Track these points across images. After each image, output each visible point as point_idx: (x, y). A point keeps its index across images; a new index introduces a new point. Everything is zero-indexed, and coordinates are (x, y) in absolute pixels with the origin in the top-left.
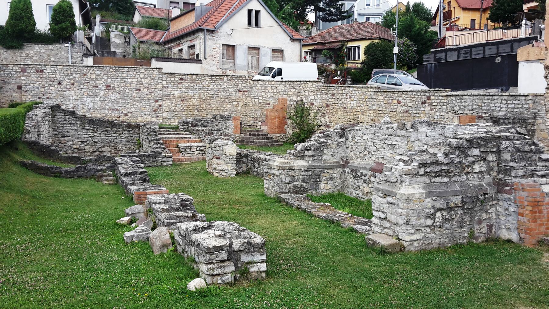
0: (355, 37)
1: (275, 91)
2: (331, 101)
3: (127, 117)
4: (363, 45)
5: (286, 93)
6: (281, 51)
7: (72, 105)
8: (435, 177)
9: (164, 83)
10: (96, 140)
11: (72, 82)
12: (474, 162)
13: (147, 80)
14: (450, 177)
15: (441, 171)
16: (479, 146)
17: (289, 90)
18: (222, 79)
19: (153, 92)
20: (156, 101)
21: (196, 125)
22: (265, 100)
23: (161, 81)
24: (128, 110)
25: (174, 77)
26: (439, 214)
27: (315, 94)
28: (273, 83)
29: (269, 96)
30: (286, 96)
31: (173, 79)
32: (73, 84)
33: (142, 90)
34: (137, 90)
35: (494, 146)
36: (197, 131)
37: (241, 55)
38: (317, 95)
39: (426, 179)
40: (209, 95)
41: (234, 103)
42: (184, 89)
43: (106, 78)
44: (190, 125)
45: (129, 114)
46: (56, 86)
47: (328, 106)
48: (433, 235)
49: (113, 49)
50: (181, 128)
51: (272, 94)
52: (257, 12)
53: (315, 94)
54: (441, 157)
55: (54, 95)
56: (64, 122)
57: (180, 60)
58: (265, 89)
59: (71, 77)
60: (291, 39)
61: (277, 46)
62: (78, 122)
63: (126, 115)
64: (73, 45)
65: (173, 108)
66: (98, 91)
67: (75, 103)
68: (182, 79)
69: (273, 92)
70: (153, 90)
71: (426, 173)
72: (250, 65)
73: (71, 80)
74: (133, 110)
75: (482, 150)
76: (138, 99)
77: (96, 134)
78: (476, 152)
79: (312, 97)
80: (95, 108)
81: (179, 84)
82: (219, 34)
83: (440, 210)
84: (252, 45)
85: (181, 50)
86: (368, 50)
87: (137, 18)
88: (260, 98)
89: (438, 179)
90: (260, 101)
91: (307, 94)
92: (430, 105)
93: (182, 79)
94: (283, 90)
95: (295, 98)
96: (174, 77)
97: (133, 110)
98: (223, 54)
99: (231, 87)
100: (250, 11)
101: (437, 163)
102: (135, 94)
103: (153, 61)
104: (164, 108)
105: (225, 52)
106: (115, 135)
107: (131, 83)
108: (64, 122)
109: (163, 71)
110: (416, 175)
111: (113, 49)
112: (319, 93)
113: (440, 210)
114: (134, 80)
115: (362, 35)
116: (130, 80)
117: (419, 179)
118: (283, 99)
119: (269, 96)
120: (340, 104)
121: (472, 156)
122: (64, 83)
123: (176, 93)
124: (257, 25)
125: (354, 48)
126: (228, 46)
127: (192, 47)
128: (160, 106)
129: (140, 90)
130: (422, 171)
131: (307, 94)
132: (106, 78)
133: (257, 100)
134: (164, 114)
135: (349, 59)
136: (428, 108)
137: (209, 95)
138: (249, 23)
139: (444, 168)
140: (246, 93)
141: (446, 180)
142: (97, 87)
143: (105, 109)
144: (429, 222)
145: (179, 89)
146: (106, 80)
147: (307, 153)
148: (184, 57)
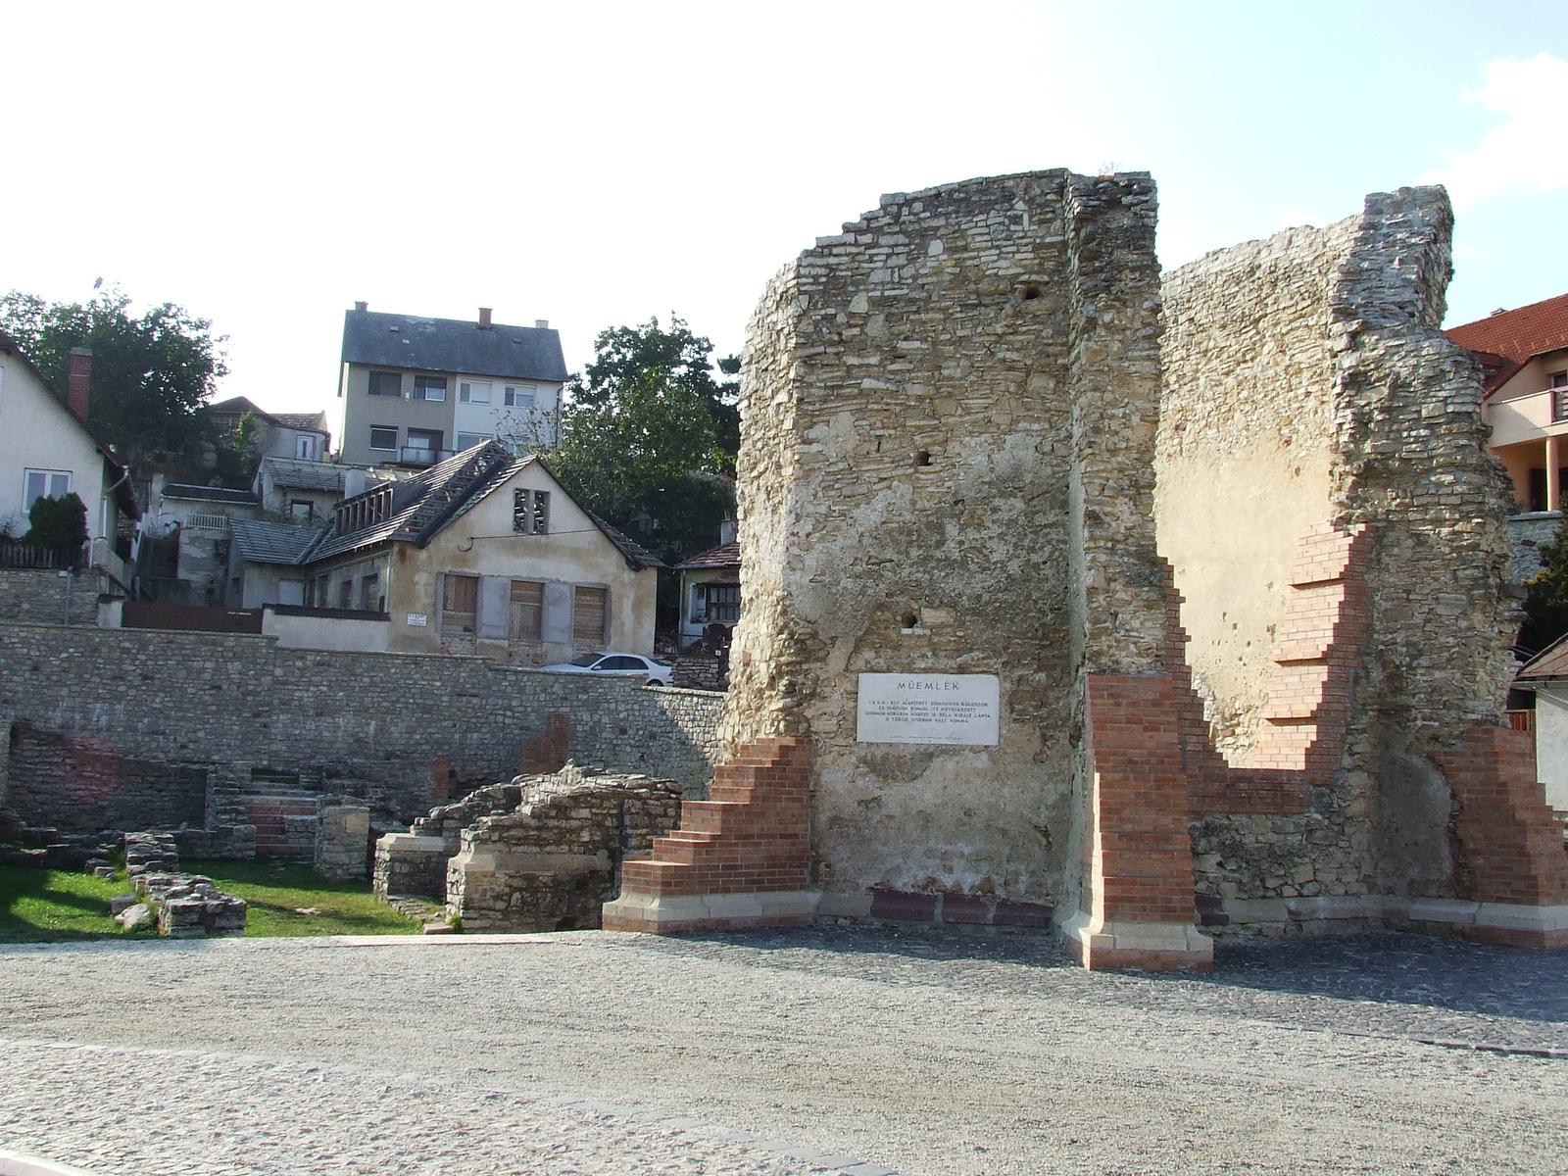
1: (542, 697)
3: (186, 751)
5: (568, 703)
6: (603, 593)
7: (59, 721)
8: (516, 845)
10: (105, 803)
11: (65, 665)
12: (582, 828)
14: (541, 846)
15: (526, 838)
19: (249, 693)
20: (257, 715)
21: (336, 775)
22: (518, 718)
23: (271, 668)
24: (190, 735)
26: (517, 895)
27: (629, 707)
28: (539, 678)
29: (530, 709)
30: (568, 709)
33: (225, 687)
34: (213, 687)
35: (615, 807)
36: (335, 786)
37: (491, 604)
38: (632, 709)
39: (500, 846)
40: (384, 704)
41: (445, 724)
42: (325, 689)
43: (144, 658)
44: (324, 774)
45: (191, 746)
46: (27, 675)
47: (653, 736)
48: (507, 923)
49: (183, 574)
50: (303, 779)
51: (535, 704)
52: (542, 497)
53: (629, 707)
55: (20, 695)
56: (37, 760)
57: (343, 612)
58: (521, 691)
59: (64, 655)
61: (591, 578)
62: (68, 761)
63: (183, 747)
65: (297, 732)
66: (122, 689)
68: (319, 664)
69: (538, 700)
70: (251, 688)
71: (501, 839)
73: (62, 660)
74: (201, 734)
75: (594, 810)
76: (214, 708)
77: (105, 789)
78: (585, 813)
80: (109, 728)
83: (519, 889)
88: (509, 713)
89: (521, 849)
91: (613, 706)
94: (561, 693)
97: (201, 734)
98: (446, 598)
99: (438, 684)
100: (520, 495)
105: (452, 595)
106: (149, 792)
108: (37, 760)
109: (279, 644)
110: (486, 840)
111: (183, 574)
112: (636, 707)
113: (519, 889)
114: (208, 665)
117: (491, 846)
118: (559, 717)
119: (530, 709)
121: (579, 819)
126: (461, 578)
127: (372, 579)
128: (265, 726)
129: (219, 688)
130: (495, 836)
131: (613, 706)
132: (144, 658)
133: (500, 719)
134: (274, 748)
137: (384, 704)
138: (519, 525)
139: (532, 833)
140: (475, 700)
141: (535, 849)
142: (122, 679)
144: (501, 905)
145: (312, 688)
146: (143, 663)
147: (446, 823)
148: (354, 608)
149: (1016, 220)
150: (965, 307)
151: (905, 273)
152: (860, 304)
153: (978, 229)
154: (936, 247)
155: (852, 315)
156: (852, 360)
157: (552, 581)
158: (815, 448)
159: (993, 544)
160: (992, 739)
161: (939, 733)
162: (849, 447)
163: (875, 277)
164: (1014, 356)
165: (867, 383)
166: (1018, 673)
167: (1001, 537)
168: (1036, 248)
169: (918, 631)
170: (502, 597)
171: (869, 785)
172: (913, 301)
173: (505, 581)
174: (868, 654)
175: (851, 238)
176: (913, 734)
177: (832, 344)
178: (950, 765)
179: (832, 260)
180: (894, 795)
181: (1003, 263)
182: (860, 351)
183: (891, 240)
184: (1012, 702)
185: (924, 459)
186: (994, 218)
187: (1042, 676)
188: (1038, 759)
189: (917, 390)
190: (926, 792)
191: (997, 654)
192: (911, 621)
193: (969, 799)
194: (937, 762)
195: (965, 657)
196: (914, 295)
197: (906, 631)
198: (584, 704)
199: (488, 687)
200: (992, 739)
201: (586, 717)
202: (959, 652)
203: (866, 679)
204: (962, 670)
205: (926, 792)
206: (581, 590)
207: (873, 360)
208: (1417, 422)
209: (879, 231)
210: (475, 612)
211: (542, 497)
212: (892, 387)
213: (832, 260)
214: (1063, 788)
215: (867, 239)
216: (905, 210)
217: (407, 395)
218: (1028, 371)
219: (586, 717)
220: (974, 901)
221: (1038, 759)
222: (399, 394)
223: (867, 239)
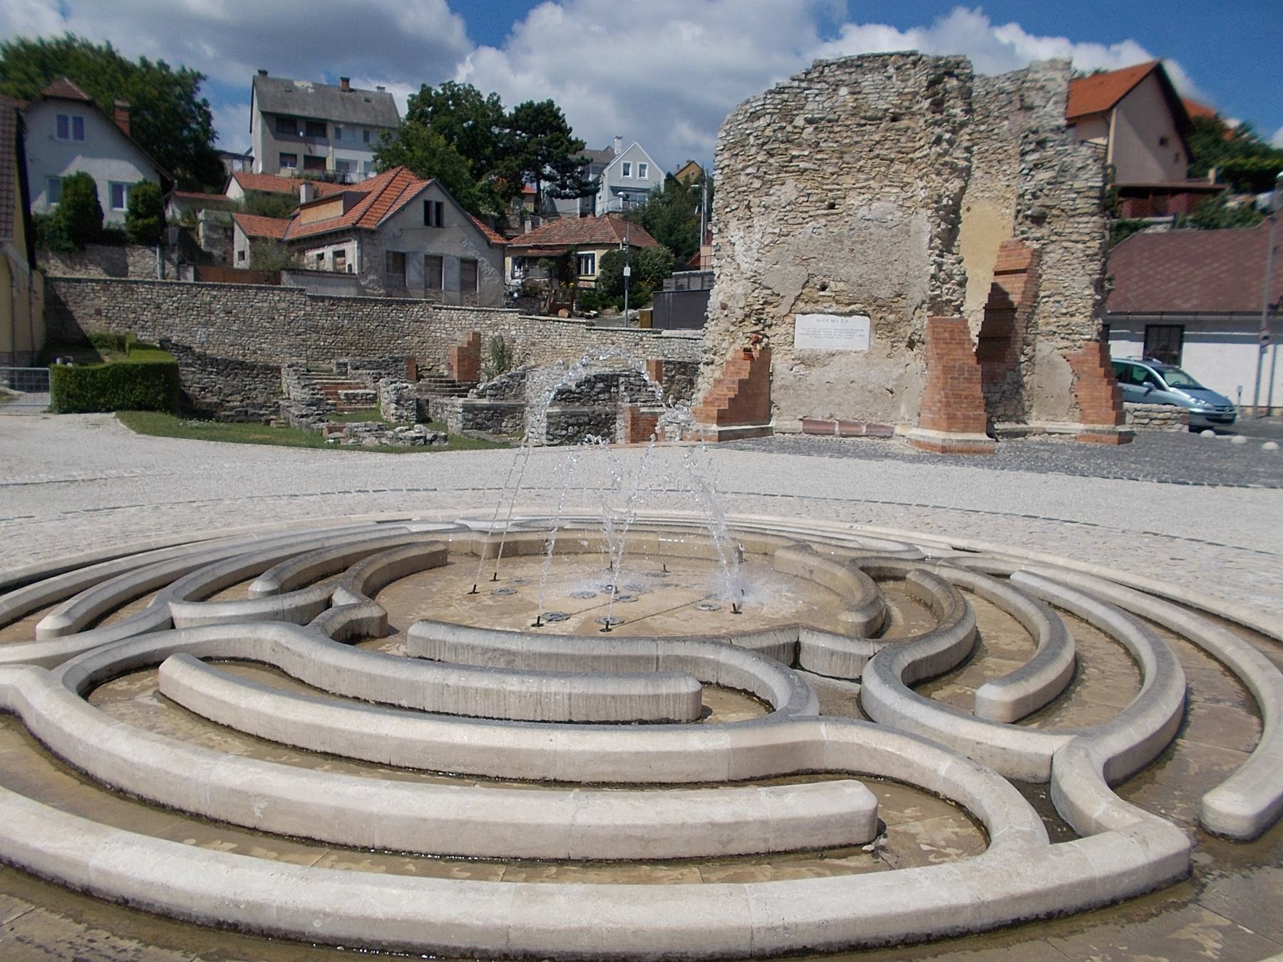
0: (587, 240)
2: (537, 338)
4: (599, 254)
6: (475, 262)
9: (308, 309)
13: (283, 305)
16: (602, 381)
32: (177, 308)
47: (533, 344)
52: (439, 205)
54: (573, 388)
58: (451, 319)
61: (471, 254)
78: (601, 385)
85: (321, 257)
86: (604, 260)
87: (234, 192)
92: (643, 347)
95: (490, 333)
101: (570, 391)
105: (391, 262)
115: (599, 238)
120: (548, 342)
122: (164, 307)
123: (325, 323)
124: (439, 223)
125: (587, 257)
135: (579, 272)
136: (641, 351)
138: (427, 221)
149: (890, 78)
150: (860, 125)
151: (826, 105)
152: (799, 121)
153: (869, 81)
154: (843, 91)
155: (795, 127)
156: (795, 153)
158: (774, 198)
159: (870, 252)
160: (865, 347)
161: (838, 344)
162: (793, 198)
163: (809, 107)
164: (885, 152)
165: (802, 165)
166: (879, 315)
167: (874, 248)
168: (899, 94)
169: (826, 293)
171: (800, 369)
172: (829, 121)
174: (801, 305)
175: (796, 84)
176: (823, 346)
177: (782, 142)
178: (844, 360)
179: (786, 96)
180: (815, 374)
181: (881, 102)
182: (800, 145)
183: (819, 86)
184: (875, 328)
185: (832, 206)
186: (878, 77)
187: (892, 317)
188: (889, 356)
189: (831, 169)
190: (831, 373)
191: (870, 305)
192: (824, 288)
193: (853, 376)
194: (835, 359)
195: (852, 307)
196: (831, 116)
197: (822, 293)
198: (489, 326)
200: (865, 347)
202: (849, 304)
203: (799, 317)
204: (851, 313)
205: (831, 373)
206: (464, 261)
207: (806, 153)
208: (1071, 189)
209: (811, 81)
211: (439, 205)
212: (815, 167)
213: (786, 96)
214: (902, 371)
215: (804, 85)
216: (827, 70)
218: (892, 161)
219: (490, 333)
220: (855, 425)
221: (889, 356)
222: (325, 136)
223: (804, 85)
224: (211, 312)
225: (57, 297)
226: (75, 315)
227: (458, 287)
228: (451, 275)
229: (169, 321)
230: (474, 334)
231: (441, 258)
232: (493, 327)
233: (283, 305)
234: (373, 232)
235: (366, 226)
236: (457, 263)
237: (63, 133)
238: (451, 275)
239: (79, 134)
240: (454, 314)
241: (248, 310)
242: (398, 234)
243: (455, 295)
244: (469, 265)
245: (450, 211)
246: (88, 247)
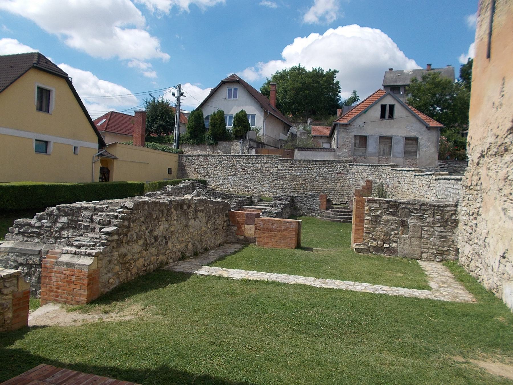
6: (416, 139)
9: (279, 166)
13: (268, 165)
17: (374, 173)
18: (324, 164)
25: (287, 162)
28: (363, 167)
31: (286, 164)
32: (223, 168)
52: (392, 107)
60: (427, 127)
64: (243, 141)
67: (223, 180)
72: (382, 152)
74: (257, 186)
79: (388, 180)
81: (291, 167)
82: (352, 127)
84: (384, 134)
90: (353, 183)
91: (385, 177)
93: (292, 164)
96: (287, 162)
100: (383, 107)
102: (260, 175)
103: (296, 151)
104: (278, 185)
105: (358, 141)
107: (257, 167)
114: (259, 165)
116: (257, 165)
122: (218, 167)
123: (287, 174)
126: (361, 137)
143: (240, 185)
157: (395, 136)
170: (376, 142)
173: (377, 136)
199: (347, 171)
201: (378, 181)
206: (407, 139)
210: (366, 147)
217: (401, 93)
224: (236, 169)
225: (182, 163)
226: (187, 171)
227: (402, 155)
228: (398, 148)
229: (220, 174)
230: (368, 181)
231: (391, 138)
232: (379, 176)
233: (268, 165)
234: (346, 125)
235: (342, 122)
236: (402, 142)
237: (230, 97)
238: (398, 148)
239: (235, 96)
240: (360, 168)
241: (252, 168)
242: (362, 125)
243: (400, 160)
244: (412, 141)
245: (398, 111)
246: (219, 142)
